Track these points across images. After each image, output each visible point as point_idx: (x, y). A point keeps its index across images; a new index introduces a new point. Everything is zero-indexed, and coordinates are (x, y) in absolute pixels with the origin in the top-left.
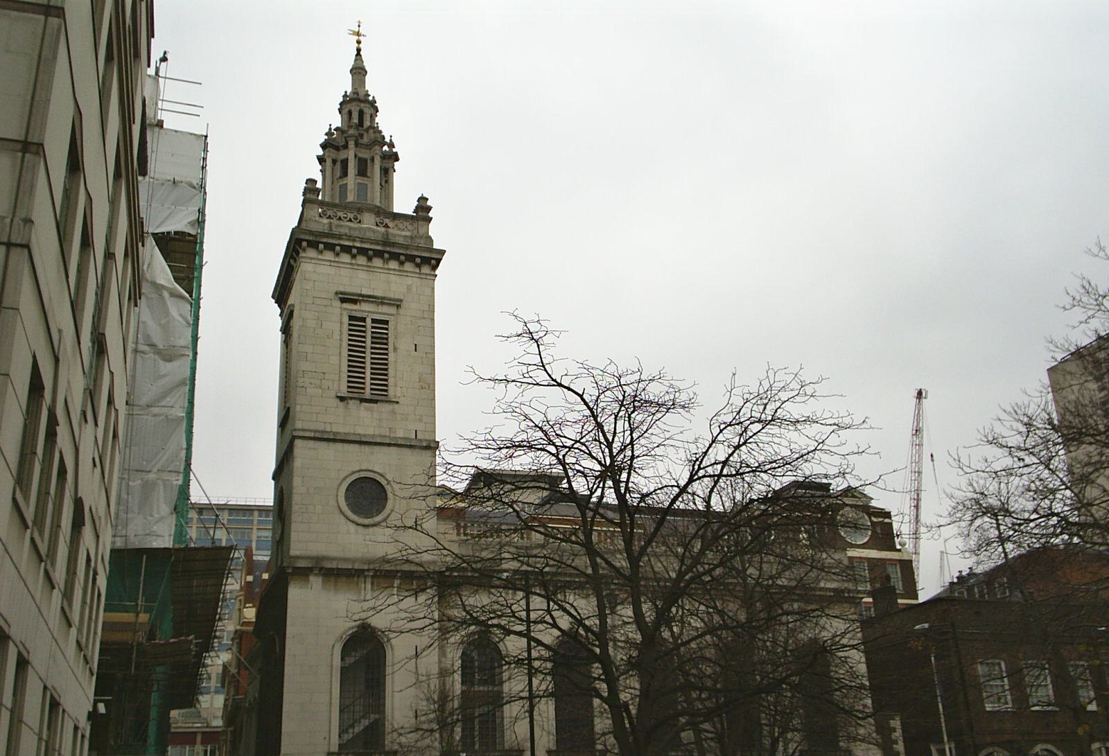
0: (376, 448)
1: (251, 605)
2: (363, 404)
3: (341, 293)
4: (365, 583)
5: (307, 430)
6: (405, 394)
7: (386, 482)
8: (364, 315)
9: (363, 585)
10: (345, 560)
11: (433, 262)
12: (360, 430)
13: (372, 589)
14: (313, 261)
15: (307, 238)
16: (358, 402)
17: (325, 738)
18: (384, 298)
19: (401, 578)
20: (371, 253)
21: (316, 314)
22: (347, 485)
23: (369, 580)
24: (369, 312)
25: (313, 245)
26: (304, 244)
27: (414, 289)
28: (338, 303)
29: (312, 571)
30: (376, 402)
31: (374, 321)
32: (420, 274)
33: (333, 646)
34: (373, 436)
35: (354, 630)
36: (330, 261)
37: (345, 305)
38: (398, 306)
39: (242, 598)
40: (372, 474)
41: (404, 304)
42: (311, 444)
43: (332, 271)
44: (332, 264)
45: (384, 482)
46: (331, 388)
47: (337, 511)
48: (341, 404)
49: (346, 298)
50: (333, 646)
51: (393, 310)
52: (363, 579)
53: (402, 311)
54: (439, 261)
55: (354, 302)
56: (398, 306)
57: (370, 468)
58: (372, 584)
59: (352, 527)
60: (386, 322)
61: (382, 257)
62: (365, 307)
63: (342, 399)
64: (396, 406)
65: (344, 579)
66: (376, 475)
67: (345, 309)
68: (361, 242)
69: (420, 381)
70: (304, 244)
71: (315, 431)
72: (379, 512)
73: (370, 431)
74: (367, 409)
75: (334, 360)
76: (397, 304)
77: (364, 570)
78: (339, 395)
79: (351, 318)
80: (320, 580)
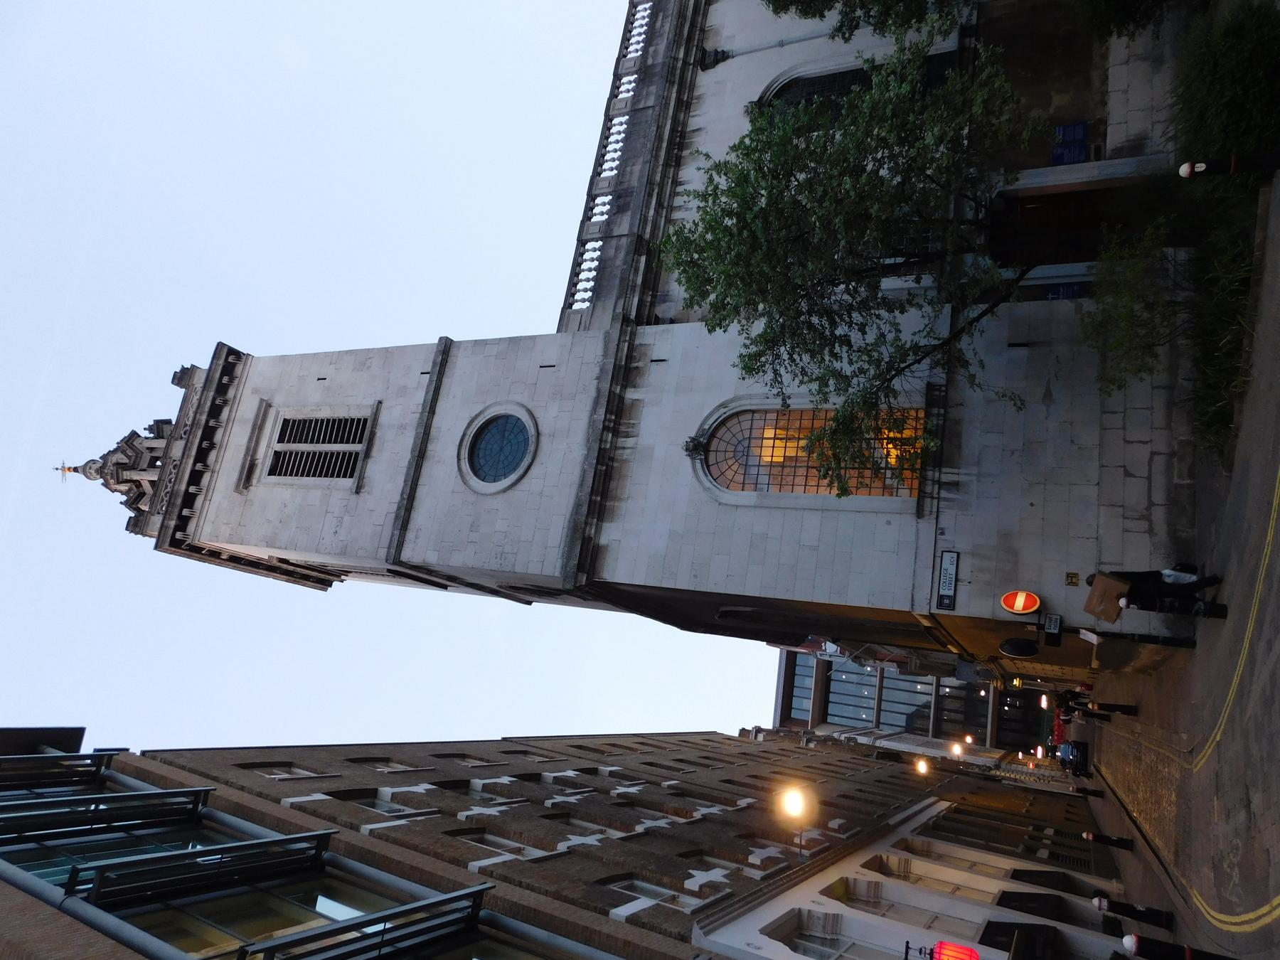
1: (823, 644)
3: (237, 486)
4: (624, 448)
5: (391, 540)
8: (271, 454)
9: (628, 451)
10: (581, 484)
11: (231, 359)
12: (404, 463)
15: (171, 531)
17: (889, 523)
19: (624, 387)
20: (205, 444)
22: (475, 478)
23: (621, 441)
24: (268, 446)
25: (183, 523)
26: (179, 535)
29: (590, 539)
30: (373, 434)
31: (281, 440)
35: (698, 465)
36: (205, 500)
39: (818, 653)
42: (410, 535)
44: (209, 498)
47: (510, 493)
52: (620, 452)
54: (232, 352)
57: (458, 443)
58: (627, 436)
60: (286, 422)
61: (214, 429)
65: (613, 485)
66: (469, 432)
70: (179, 535)
72: (523, 428)
76: (266, 406)
77: (600, 449)
79: (272, 472)
80: (606, 525)
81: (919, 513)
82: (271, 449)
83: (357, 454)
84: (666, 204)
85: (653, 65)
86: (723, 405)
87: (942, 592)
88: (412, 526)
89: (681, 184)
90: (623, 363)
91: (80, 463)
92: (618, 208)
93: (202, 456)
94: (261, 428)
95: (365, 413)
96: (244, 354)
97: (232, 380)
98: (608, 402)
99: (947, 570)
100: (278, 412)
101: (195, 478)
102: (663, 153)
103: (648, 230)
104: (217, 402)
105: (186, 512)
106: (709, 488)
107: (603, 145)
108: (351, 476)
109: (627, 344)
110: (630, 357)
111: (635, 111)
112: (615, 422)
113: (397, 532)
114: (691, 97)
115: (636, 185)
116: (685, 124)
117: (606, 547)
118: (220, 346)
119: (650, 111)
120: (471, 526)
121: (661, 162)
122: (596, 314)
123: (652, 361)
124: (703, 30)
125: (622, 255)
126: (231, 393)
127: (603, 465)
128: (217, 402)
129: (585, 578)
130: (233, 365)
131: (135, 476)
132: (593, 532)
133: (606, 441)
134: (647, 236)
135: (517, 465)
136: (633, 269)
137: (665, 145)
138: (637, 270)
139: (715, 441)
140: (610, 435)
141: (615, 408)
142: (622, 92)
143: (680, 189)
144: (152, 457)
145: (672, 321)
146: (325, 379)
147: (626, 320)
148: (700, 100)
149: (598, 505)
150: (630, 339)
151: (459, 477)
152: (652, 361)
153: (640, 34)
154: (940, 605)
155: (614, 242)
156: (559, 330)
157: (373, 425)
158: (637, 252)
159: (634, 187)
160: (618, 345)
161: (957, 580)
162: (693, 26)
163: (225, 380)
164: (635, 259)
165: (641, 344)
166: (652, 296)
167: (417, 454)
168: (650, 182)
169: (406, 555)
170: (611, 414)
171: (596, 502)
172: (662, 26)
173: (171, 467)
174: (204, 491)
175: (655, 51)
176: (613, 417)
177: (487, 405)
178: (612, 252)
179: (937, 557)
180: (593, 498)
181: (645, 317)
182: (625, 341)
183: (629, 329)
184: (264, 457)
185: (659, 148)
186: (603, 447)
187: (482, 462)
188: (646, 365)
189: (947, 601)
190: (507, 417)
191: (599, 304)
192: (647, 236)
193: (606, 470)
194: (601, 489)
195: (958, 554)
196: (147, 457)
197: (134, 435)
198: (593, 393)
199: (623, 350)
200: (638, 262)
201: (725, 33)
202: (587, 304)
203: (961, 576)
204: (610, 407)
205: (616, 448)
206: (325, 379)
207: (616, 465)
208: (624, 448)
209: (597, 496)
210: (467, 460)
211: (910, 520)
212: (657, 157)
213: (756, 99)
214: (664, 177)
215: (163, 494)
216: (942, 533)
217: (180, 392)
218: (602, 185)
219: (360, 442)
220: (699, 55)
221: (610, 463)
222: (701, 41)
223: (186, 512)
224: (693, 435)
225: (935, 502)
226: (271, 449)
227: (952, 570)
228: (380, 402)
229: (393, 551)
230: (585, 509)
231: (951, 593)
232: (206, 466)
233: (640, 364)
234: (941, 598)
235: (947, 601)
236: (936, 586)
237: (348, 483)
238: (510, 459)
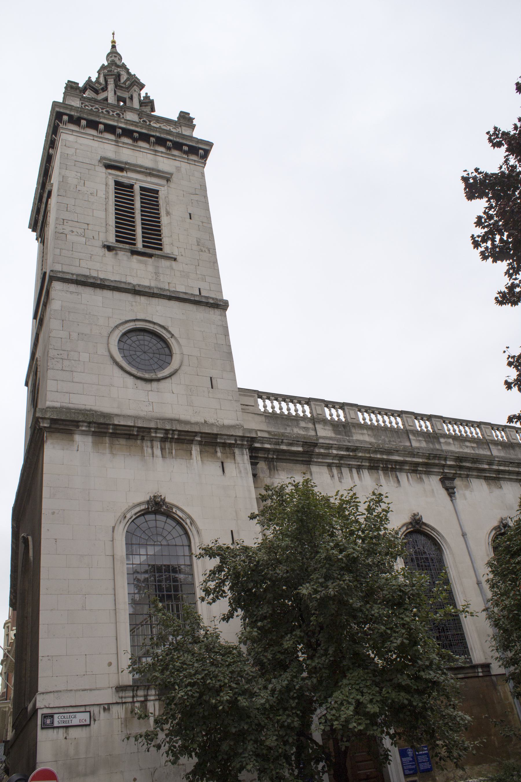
0: (155, 301)
2: (135, 257)
4: (152, 447)
5: (68, 273)
6: (183, 254)
7: (169, 336)
8: (132, 182)
9: (150, 450)
11: (201, 151)
12: (130, 280)
13: (163, 457)
14: (74, 134)
15: (68, 112)
16: (129, 254)
17: (110, 664)
18: (153, 169)
19: (200, 443)
20: (136, 135)
21: (79, 174)
22: (121, 333)
23: (157, 445)
24: (137, 180)
25: (75, 121)
26: (65, 118)
27: (183, 170)
28: (103, 169)
29: (78, 427)
30: (150, 256)
31: (142, 189)
32: (188, 159)
33: (114, 528)
34: (149, 287)
35: (143, 507)
36: (93, 136)
37: (110, 171)
38: (168, 180)
40: (152, 325)
41: (174, 178)
42: (73, 287)
43: (95, 144)
44: (95, 139)
45: (166, 335)
46: (96, 237)
48: (109, 255)
49: (110, 166)
50: (114, 528)
51: (164, 182)
52: (149, 444)
53: (172, 185)
55: (121, 169)
56: (168, 180)
57: (147, 319)
58: (162, 449)
59: (130, 380)
60: (157, 192)
61: (148, 142)
62: (131, 175)
63: (109, 248)
64: (173, 263)
65: (123, 441)
66: (156, 327)
67: (110, 174)
68: (126, 123)
69: (198, 245)
70: (65, 118)
71: (78, 275)
72: (162, 368)
73: (146, 283)
74: (140, 262)
75: (102, 214)
78: (106, 243)
79: (117, 183)
80: (89, 439)
81: (120, 689)
82: (134, 181)
83: (134, 244)
84: (342, 462)
85: (440, 443)
86: (192, 522)
87: (56, 716)
88: (80, 289)
89: (358, 473)
90: (218, 441)
91: (119, 49)
92: (336, 425)
93: (127, 133)
94: (150, 175)
95: (167, 249)
96: (206, 161)
97: (185, 153)
98: (188, 432)
99: (75, 717)
100: (163, 186)
101: (110, 129)
102: (379, 456)
103: (322, 451)
104: (168, 143)
105: (83, 122)
106: (125, 517)
107: (277, 397)
108: (117, 241)
109: (233, 442)
110: (224, 445)
111: (407, 433)
112: (172, 438)
113: (75, 277)
114: (421, 472)
115: (354, 438)
116: (401, 470)
117: (73, 441)
118: (211, 145)
119: (408, 444)
120: (83, 334)
121: (372, 455)
122: (256, 416)
123: (222, 463)
124: (468, 476)
125: (302, 432)
126: (176, 152)
127: (138, 431)
128: (168, 143)
129: (46, 425)
130: (197, 154)
131: (111, 87)
132: (84, 428)
133: (156, 432)
134: (317, 450)
135: (133, 366)
136: (291, 442)
137: (385, 457)
138: (291, 444)
139: (163, 518)
140: (162, 436)
141: (183, 437)
142: (330, 410)
143: (354, 471)
144: (125, 99)
145: (254, 475)
146: (191, 218)
147: (253, 440)
148: (419, 480)
149: (105, 430)
150: (238, 444)
151: (121, 322)
152: (222, 463)
153: (460, 431)
154: (45, 716)
155: (310, 425)
156: (240, 390)
157: (158, 255)
158: (305, 444)
159: (352, 437)
160: (232, 435)
161: (67, 727)
162: (469, 469)
163: (186, 148)
164: (299, 443)
165: (234, 453)
166: (273, 458)
167: (137, 288)
168: (355, 449)
169: (57, 285)
170: (179, 435)
171: (108, 429)
172: (467, 447)
173: (118, 112)
174: (100, 135)
175: (449, 444)
176: (176, 437)
177: (179, 340)
178: (303, 424)
179: (85, 708)
180: (111, 427)
181: (257, 455)
182: (236, 440)
183: (245, 443)
184: (126, 177)
185: (382, 453)
186: (152, 430)
187: (134, 338)
188: (218, 458)
189: (48, 721)
190: (171, 354)
191: (263, 418)
192: (317, 450)
193: (134, 435)
194: (118, 432)
195: (89, 725)
196: (126, 95)
197: (142, 86)
198: (193, 420)
199: (229, 439)
200: (297, 445)
201: (467, 493)
202: (262, 409)
203: (71, 731)
204: (183, 433)
205: (152, 441)
206: (191, 218)
207: (139, 442)
208: (152, 447)
209: (113, 429)
210: (135, 327)
211: (114, 683)
212: (375, 452)
213: (424, 520)
214: (362, 458)
215: (97, 106)
216: (104, 709)
217: (175, 117)
218: (352, 412)
219: (144, 246)
220: (451, 476)
221: (140, 437)
222: (460, 476)
223: (83, 122)
224: (167, 500)
225: (130, 700)
226: (134, 181)
227: (75, 722)
228: (175, 259)
229: (60, 275)
230: (102, 421)
231: (56, 724)
232: (119, 136)
233: (219, 454)
234: (51, 716)
235: (48, 721)
236: (61, 710)
237: (112, 239)
238: (138, 360)
